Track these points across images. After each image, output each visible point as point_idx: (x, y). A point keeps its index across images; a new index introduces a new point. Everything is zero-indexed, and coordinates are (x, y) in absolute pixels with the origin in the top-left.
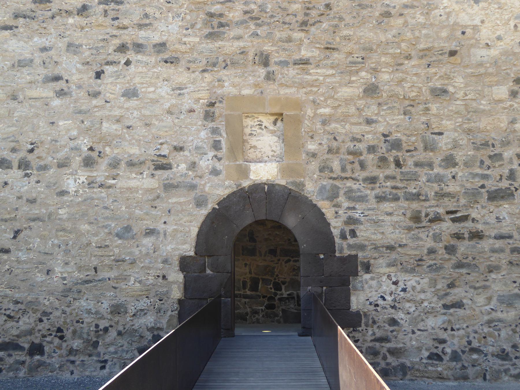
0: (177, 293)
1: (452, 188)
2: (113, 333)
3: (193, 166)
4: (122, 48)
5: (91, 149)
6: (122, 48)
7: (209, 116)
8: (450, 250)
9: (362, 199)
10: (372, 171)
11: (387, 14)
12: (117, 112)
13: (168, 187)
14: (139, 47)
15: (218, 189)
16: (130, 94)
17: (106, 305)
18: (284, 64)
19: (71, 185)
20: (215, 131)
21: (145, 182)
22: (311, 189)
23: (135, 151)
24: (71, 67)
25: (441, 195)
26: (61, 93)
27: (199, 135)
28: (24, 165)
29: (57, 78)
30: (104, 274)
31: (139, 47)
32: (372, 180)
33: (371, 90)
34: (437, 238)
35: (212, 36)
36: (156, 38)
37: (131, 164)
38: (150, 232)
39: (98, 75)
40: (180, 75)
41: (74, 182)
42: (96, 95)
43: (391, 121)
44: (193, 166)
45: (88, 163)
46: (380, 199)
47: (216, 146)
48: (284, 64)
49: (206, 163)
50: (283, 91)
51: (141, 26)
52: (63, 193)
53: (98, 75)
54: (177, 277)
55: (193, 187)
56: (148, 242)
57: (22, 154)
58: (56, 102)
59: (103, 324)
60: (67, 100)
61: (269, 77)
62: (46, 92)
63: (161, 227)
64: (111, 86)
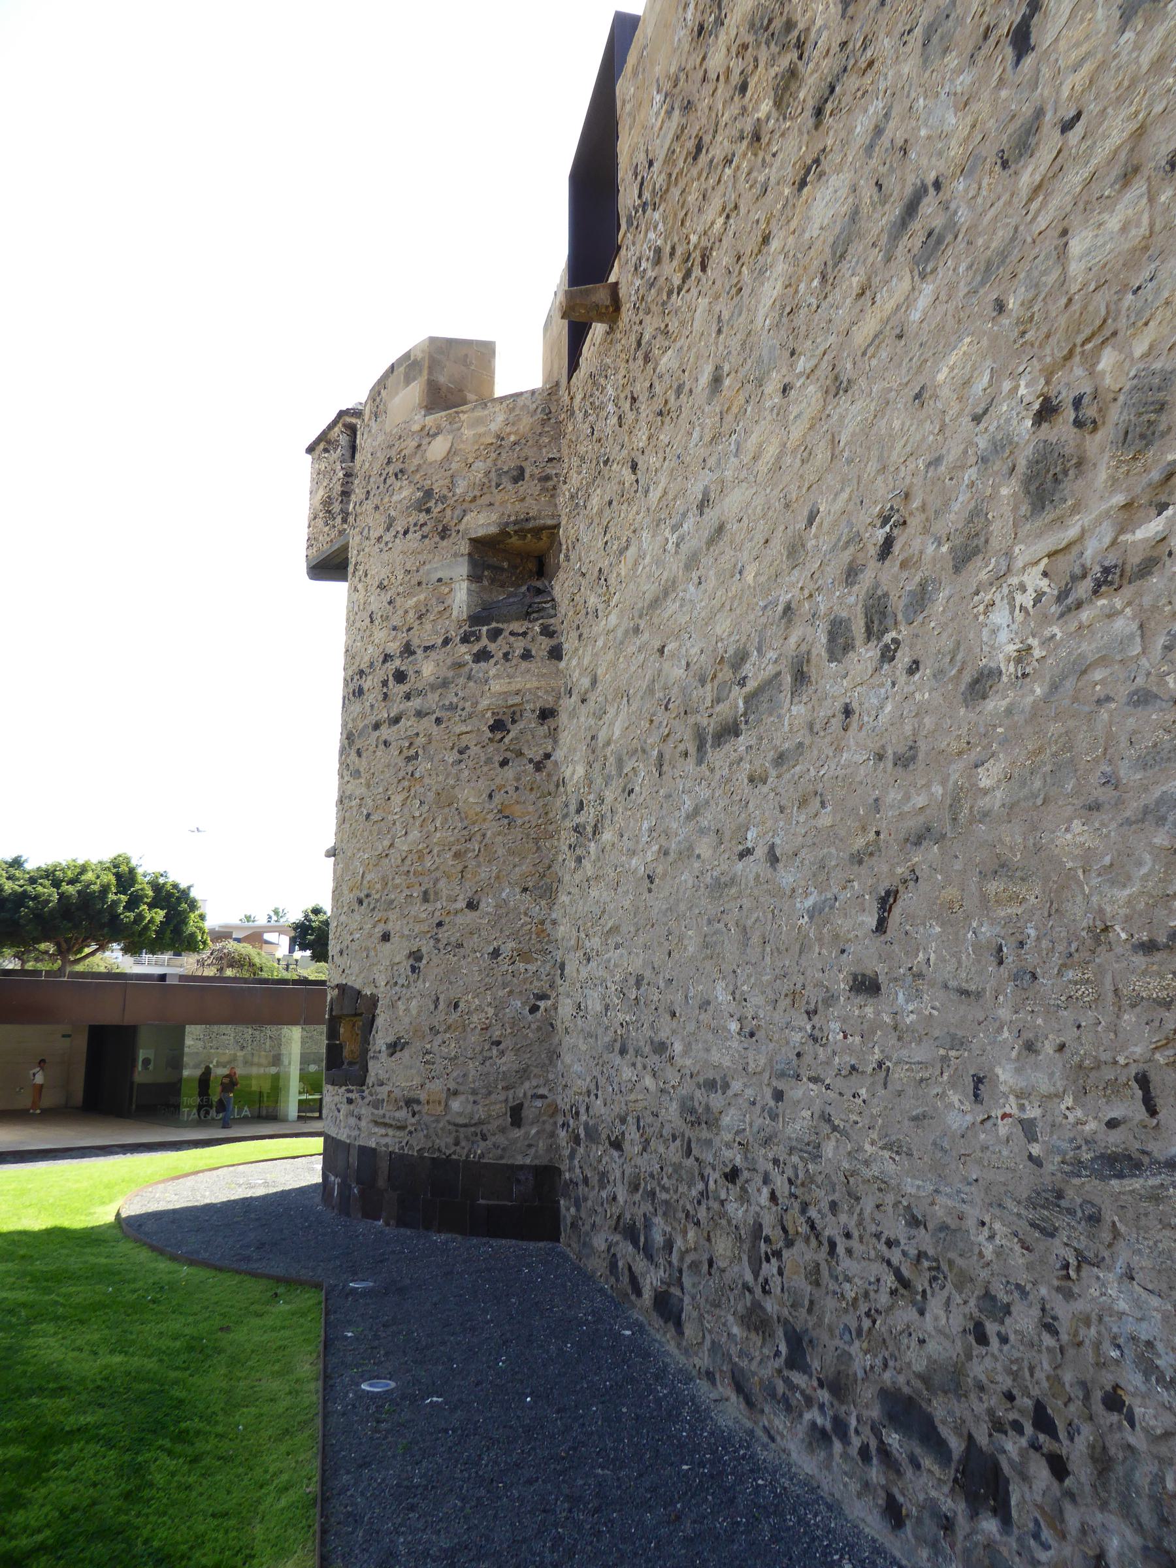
5: (1046, 412)
19: (1001, 634)
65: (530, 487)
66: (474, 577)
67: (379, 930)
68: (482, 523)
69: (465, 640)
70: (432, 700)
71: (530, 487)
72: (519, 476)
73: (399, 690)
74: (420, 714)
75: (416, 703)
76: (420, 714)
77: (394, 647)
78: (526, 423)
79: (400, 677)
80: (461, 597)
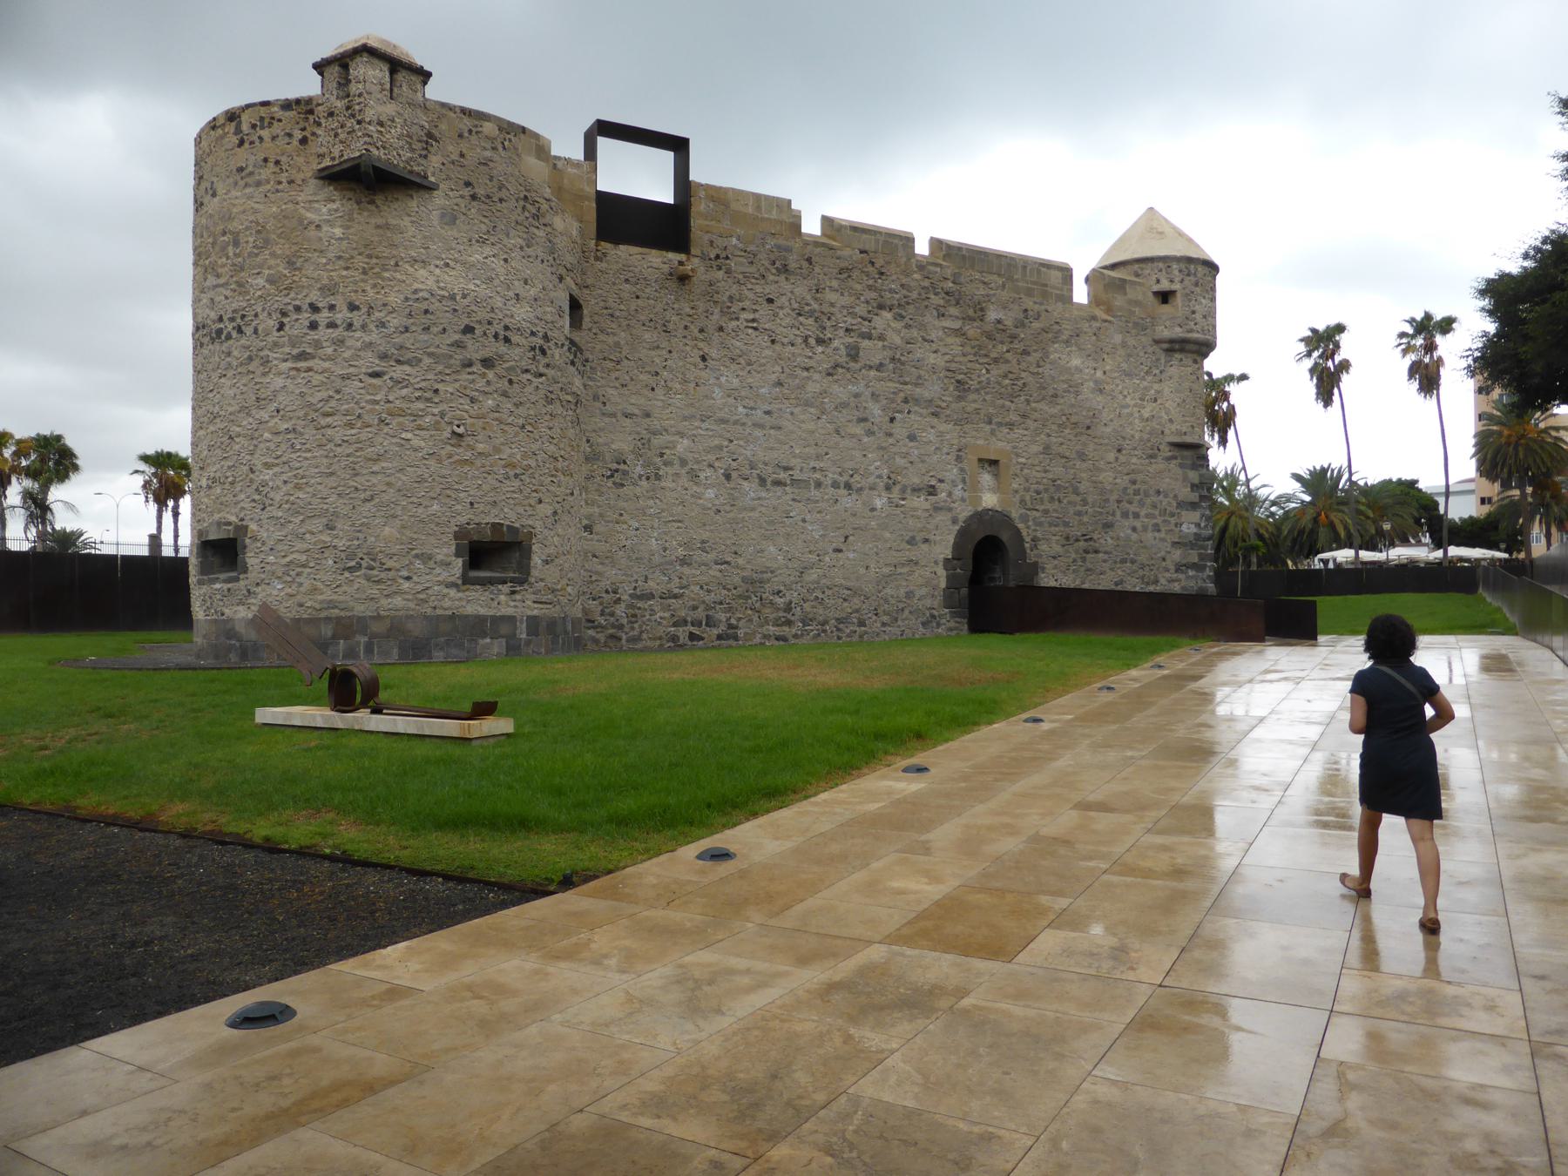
0: (943, 585)
1: (1085, 519)
2: (906, 612)
3: (950, 494)
4: (906, 401)
6: (906, 401)
7: (959, 459)
8: (1084, 560)
9: (1040, 524)
10: (1048, 506)
11: (1055, 396)
12: (904, 450)
13: (937, 509)
14: (917, 401)
15: (964, 512)
16: (912, 438)
17: (902, 591)
18: (1000, 424)
20: (962, 470)
21: (920, 502)
22: (1015, 514)
23: (916, 480)
24: (875, 410)
25: (1081, 523)
26: (870, 433)
27: (953, 473)
28: (848, 486)
29: (865, 420)
30: (899, 570)
31: (917, 401)
32: (1046, 512)
33: (1047, 449)
34: (1077, 552)
35: (960, 398)
36: (927, 395)
37: (914, 490)
38: (926, 541)
39: (892, 420)
40: (943, 427)
41: (878, 503)
42: (890, 435)
43: (1057, 470)
44: (950, 494)
45: (888, 488)
46: (1051, 525)
47: (964, 481)
48: (1000, 424)
49: (958, 493)
50: (1000, 444)
51: (916, 385)
52: (873, 510)
53: (892, 420)
54: (942, 573)
55: (950, 510)
56: (925, 547)
57: (846, 478)
58: (866, 440)
59: (901, 606)
60: (872, 438)
61: (993, 433)
62: (858, 430)
63: (932, 537)
64: (899, 430)
73: (544, 361)
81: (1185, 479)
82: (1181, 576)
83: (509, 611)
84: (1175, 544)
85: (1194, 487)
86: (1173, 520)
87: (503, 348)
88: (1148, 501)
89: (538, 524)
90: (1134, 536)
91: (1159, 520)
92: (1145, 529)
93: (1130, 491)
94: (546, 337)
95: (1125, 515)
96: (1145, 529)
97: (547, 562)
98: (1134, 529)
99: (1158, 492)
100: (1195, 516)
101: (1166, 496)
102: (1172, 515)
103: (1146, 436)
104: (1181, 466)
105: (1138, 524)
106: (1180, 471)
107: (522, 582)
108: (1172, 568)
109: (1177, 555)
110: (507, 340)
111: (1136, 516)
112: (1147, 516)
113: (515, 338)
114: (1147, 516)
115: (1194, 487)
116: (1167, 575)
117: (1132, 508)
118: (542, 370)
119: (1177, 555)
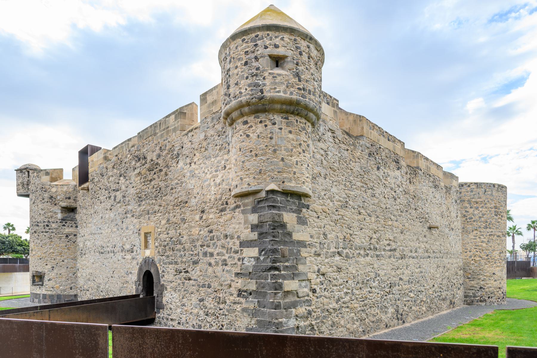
65: (72, 200)
66: (62, 213)
67: (45, 263)
68: (64, 204)
69: (60, 222)
70: (54, 230)
71: (72, 200)
72: (69, 198)
73: (48, 228)
74: (52, 232)
75: (51, 231)
76: (52, 232)
77: (46, 220)
78: (71, 190)
79: (47, 226)
80: (60, 216)
81: (246, 222)
82: (242, 300)
83: (38, 292)
84: (237, 274)
85: (254, 228)
86: (236, 256)
87: (37, 228)
88: (219, 243)
89: (46, 271)
90: (210, 270)
91: (226, 257)
92: (217, 264)
93: (208, 238)
94: (49, 222)
95: (205, 254)
96: (217, 264)
97: (49, 280)
98: (210, 264)
99: (226, 236)
100: (254, 252)
101: (232, 238)
102: (236, 252)
103: (219, 197)
104: (243, 212)
105: (212, 261)
106: (241, 216)
107: (42, 285)
108: (236, 293)
109: (240, 283)
110: (38, 226)
111: (212, 255)
112: (218, 254)
113: (40, 224)
114: (218, 254)
115: (254, 228)
116: (232, 298)
117: (210, 250)
118: (47, 230)
119: (240, 283)
